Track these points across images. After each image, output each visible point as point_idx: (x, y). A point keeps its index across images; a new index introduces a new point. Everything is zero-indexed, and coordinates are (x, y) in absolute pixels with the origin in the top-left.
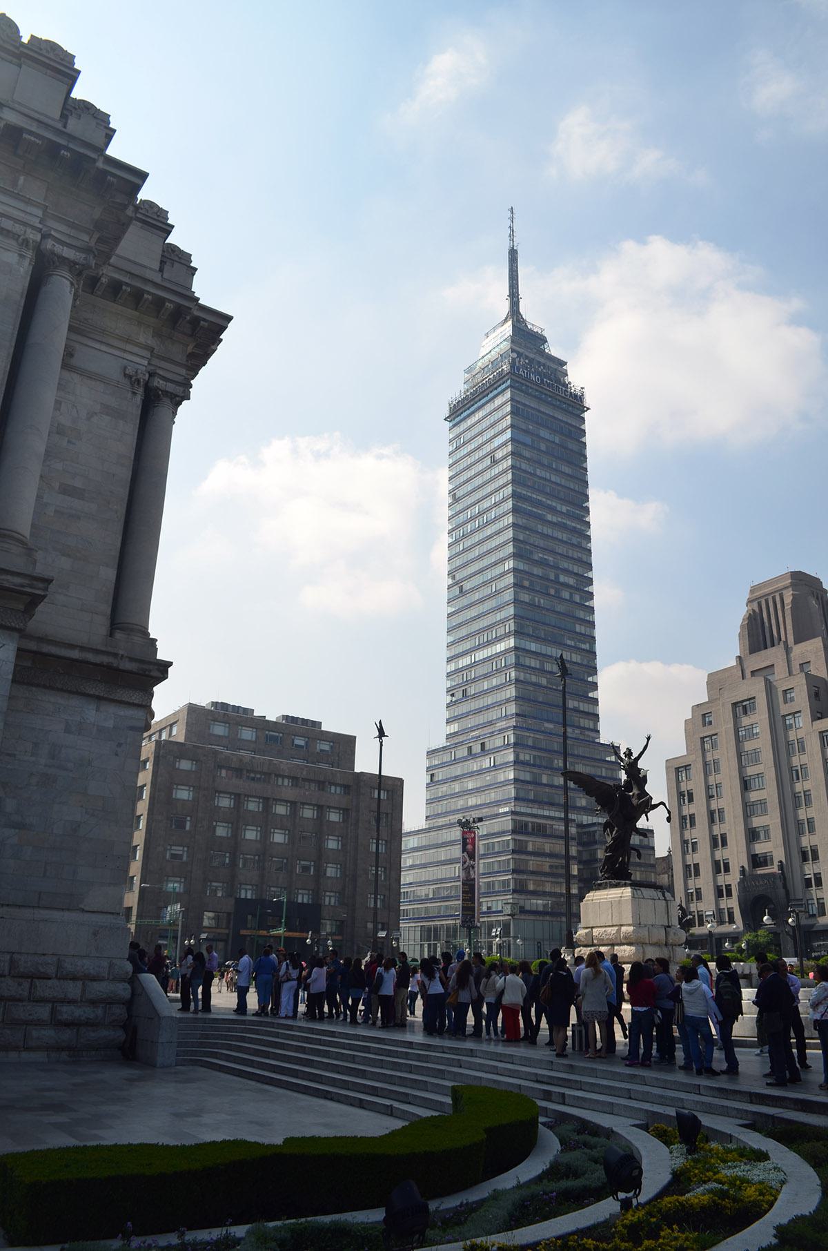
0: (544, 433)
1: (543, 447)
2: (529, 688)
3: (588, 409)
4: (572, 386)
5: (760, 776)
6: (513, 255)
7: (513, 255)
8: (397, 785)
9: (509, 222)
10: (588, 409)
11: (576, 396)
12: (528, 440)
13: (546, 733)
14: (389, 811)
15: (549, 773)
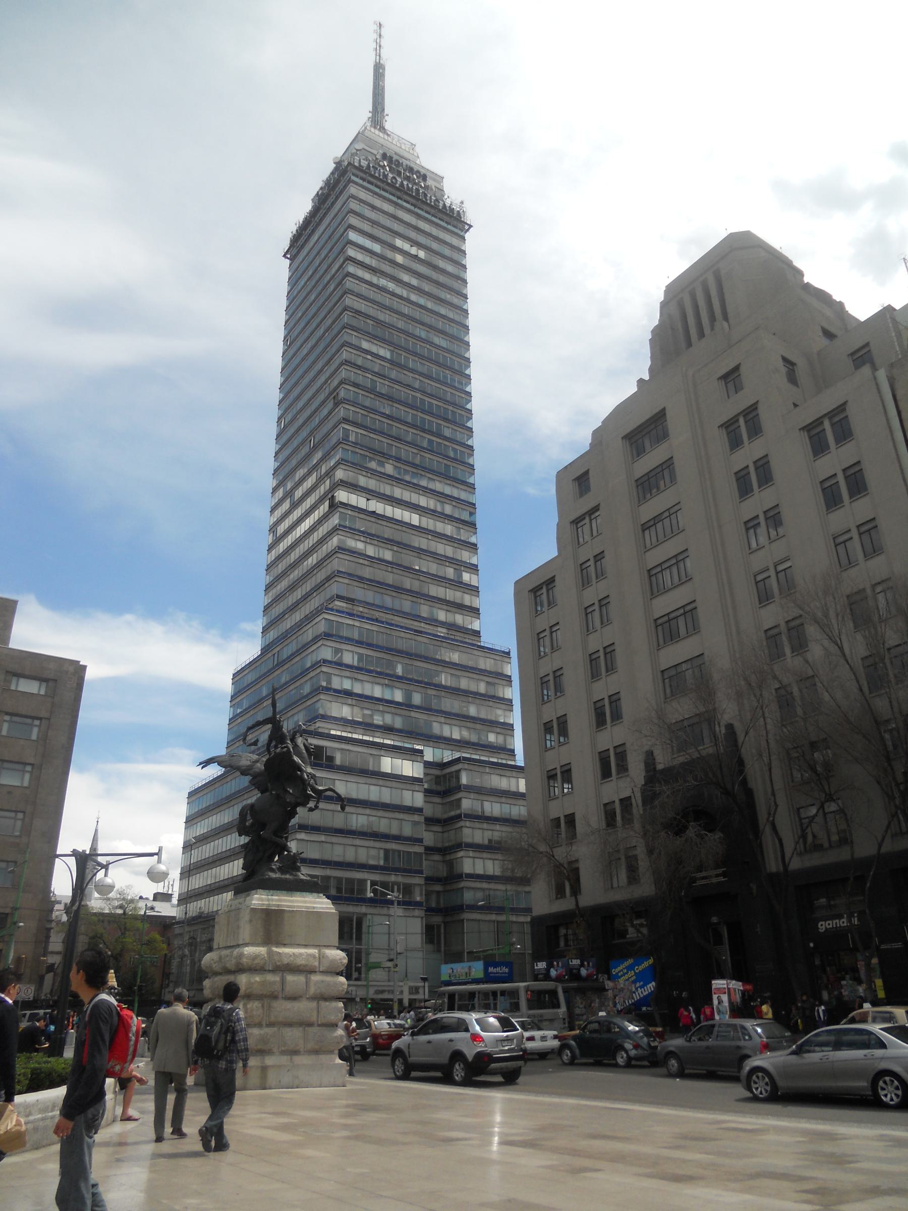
0: (399, 243)
1: (399, 259)
2: (361, 561)
3: (470, 226)
4: (446, 197)
5: (680, 557)
6: (379, 71)
7: (379, 71)
8: (67, 672)
9: (375, 36)
10: (470, 226)
11: (452, 210)
12: (377, 248)
13: (382, 622)
14: (43, 714)
15: (387, 682)
